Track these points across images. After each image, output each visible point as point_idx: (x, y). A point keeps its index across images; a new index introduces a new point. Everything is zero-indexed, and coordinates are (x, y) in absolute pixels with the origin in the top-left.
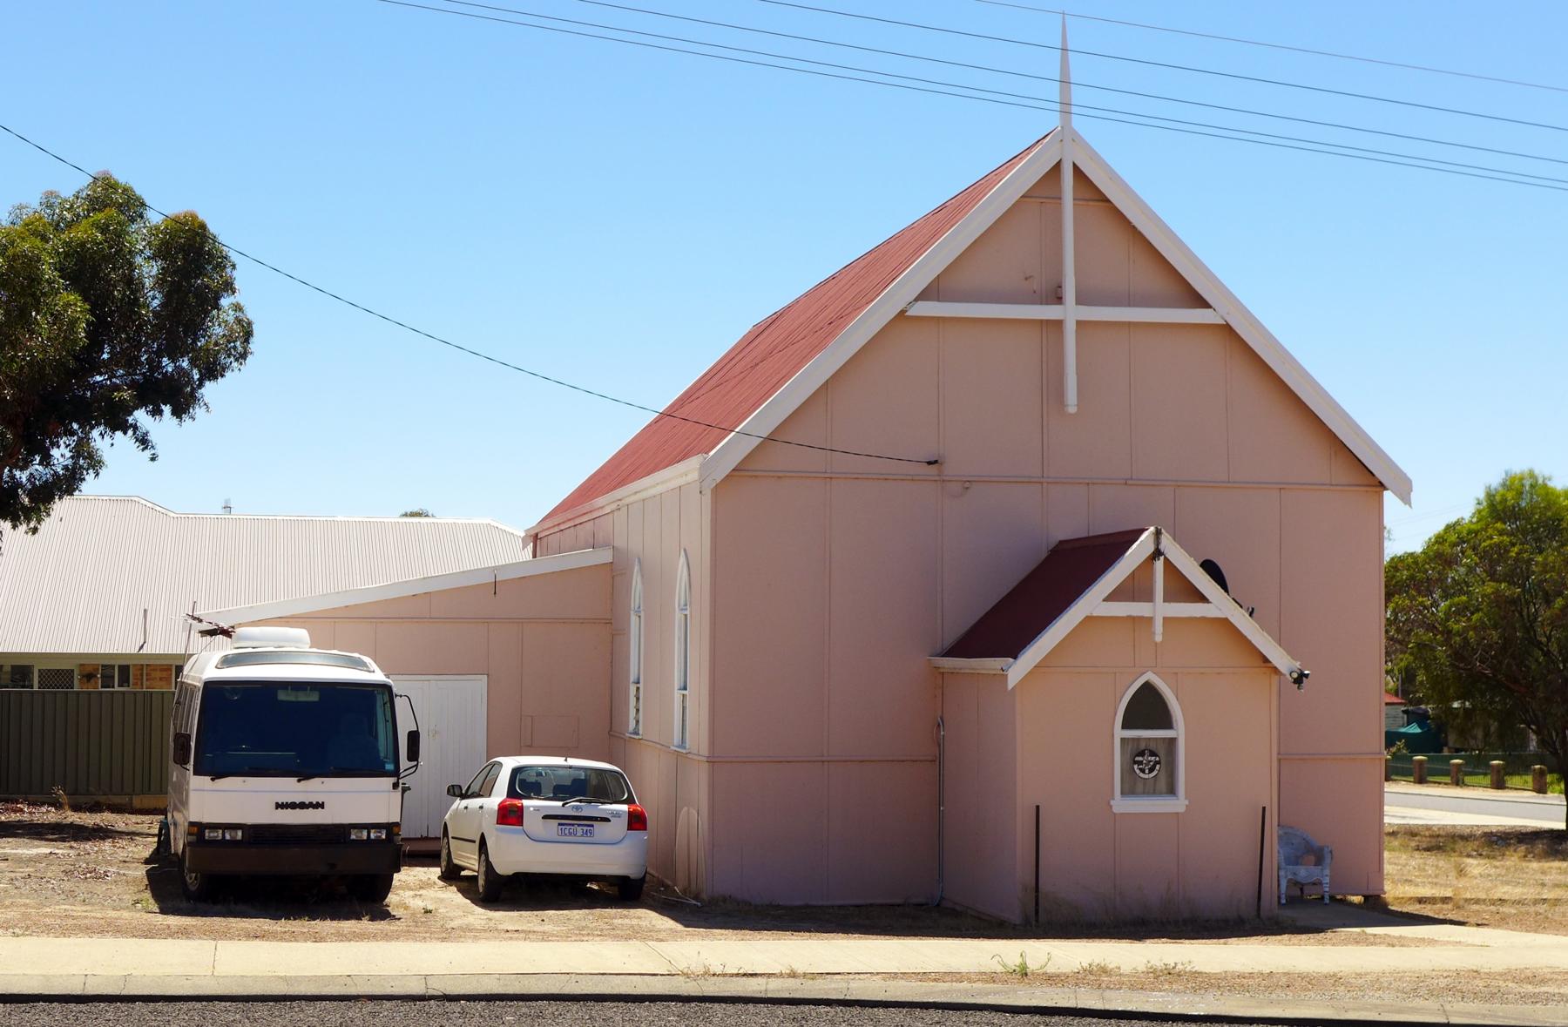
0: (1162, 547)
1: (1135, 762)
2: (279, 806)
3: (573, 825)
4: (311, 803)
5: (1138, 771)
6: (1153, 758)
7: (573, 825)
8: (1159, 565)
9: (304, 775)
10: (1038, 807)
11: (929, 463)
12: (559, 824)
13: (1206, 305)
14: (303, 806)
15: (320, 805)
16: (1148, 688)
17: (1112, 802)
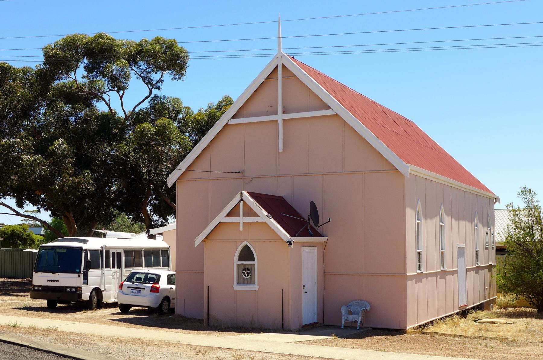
0: (243, 198)
1: (243, 273)
2: (49, 281)
3: (135, 290)
4: (55, 280)
5: (244, 276)
6: (248, 271)
7: (135, 290)
8: (241, 203)
9: (54, 272)
10: (283, 290)
11: (237, 173)
12: (132, 290)
13: (329, 108)
14: (54, 281)
15: (57, 281)
16: (246, 247)
17: (233, 286)
